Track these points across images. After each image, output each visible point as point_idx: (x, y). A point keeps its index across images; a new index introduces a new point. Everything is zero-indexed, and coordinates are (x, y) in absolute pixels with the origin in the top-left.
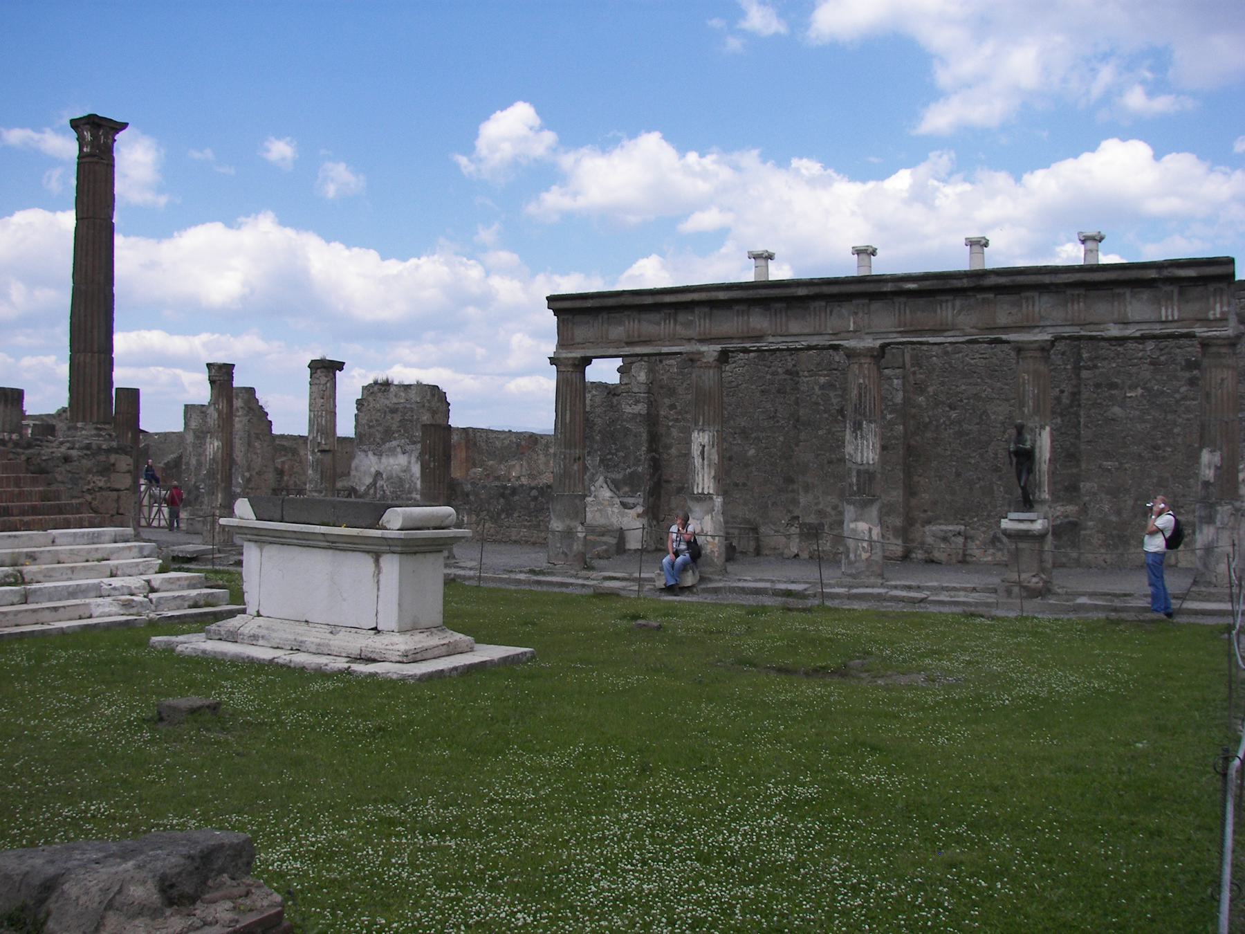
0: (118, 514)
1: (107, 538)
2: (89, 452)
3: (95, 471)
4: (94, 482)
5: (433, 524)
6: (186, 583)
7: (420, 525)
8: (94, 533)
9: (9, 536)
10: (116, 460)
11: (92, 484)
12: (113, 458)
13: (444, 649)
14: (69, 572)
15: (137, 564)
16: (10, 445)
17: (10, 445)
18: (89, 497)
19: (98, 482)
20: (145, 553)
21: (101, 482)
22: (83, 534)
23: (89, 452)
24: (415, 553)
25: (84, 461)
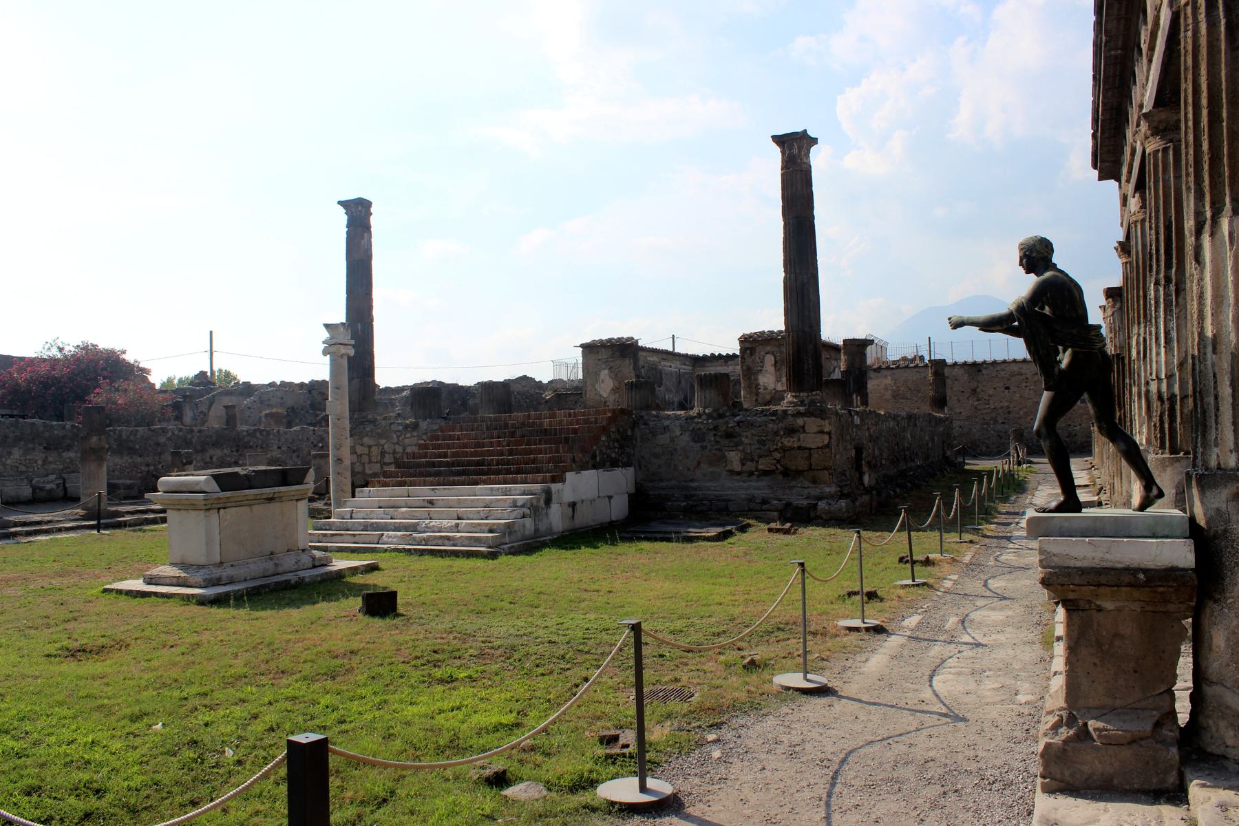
0: (810, 469)
1: (517, 492)
2: (774, 418)
3: (782, 433)
4: (782, 443)
5: (185, 490)
6: (487, 528)
7: (174, 489)
8: (506, 488)
9: (445, 489)
10: (805, 423)
11: (780, 444)
12: (800, 421)
13: (175, 581)
14: (427, 514)
15: (479, 512)
16: (704, 417)
17: (704, 417)
18: (777, 456)
19: (785, 443)
20: (519, 504)
21: (788, 442)
22: (498, 489)
23: (774, 418)
24: (180, 509)
25: (771, 426)
